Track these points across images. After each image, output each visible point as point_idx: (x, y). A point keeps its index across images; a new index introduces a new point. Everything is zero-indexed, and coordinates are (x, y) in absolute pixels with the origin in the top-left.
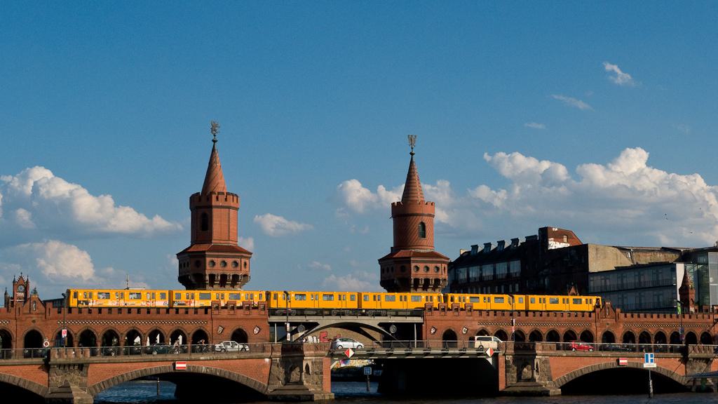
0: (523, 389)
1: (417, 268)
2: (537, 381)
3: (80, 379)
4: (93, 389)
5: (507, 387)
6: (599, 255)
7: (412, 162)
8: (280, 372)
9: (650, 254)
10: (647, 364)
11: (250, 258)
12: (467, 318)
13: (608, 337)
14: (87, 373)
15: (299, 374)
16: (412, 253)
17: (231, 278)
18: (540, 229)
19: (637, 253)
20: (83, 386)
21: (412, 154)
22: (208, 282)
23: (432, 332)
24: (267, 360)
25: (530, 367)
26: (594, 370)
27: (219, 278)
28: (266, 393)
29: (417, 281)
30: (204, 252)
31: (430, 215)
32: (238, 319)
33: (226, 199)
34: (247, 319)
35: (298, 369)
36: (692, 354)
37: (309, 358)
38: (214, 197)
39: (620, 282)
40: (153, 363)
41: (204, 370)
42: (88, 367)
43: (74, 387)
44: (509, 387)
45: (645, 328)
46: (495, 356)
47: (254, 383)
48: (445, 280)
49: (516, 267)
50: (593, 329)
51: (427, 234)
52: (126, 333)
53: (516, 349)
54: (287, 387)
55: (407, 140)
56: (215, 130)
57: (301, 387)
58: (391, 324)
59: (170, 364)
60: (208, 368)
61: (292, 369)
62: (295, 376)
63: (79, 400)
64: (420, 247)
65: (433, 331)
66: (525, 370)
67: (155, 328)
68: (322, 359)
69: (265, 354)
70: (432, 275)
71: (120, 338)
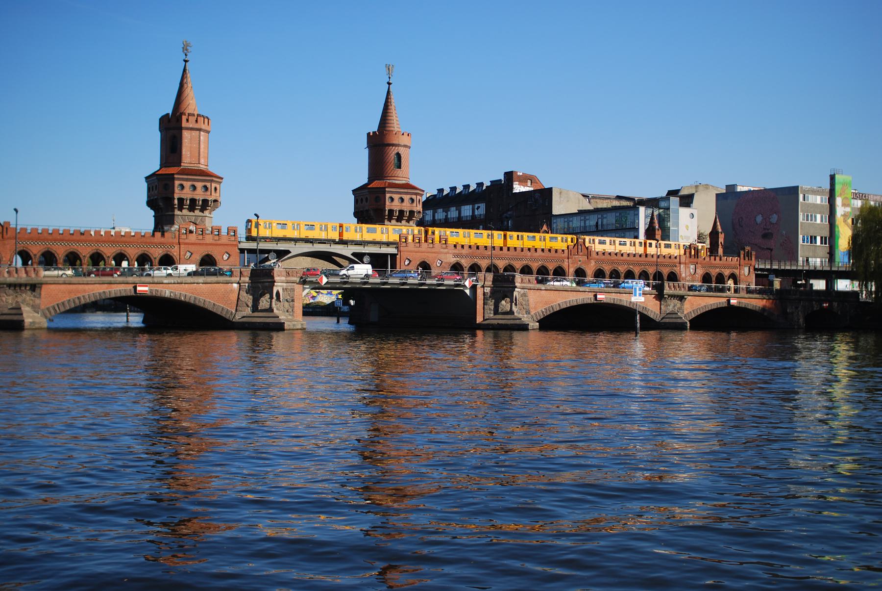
0: (501, 322)
1: (392, 199)
2: (515, 314)
3: (31, 300)
4: (47, 312)
5: (484, 320)
6: (562, 199)
7: (388, 92)
8: (248, 299)
9: (607, 201)
10: (635, 298)
11: (220, 183)
12: (442, 250)
13: (580, 273)
14: (40, 294)
15: (269, 300)
16: (387, 184)
17: (201, 202)
18: (506, 173)
19: (595, 200)
20: (35, 308)
21: (389, 84)
22: (176, 206)
23: (407, 263)
24: (236, 286)
25: (508, 299)
26: (572, 304)
27: (188, 202)
28: (234, 320)
29: (391, 211)
30: (173, 174)
31: (405, 146)
32: (206, 244)
33: (197, 121)
34: (217, 245)
35: (268, 296)
36: (667, 291)
37: (279, 284)
38: (184, 118)
39: (582, 224)
40: (113, 286)
41: (167, 295)
42: (41, 288)
43: (26, 309)
44: (487, 319)
45: (616, 266)
46: (474, 288)
47: (221, 309)
48: (419, 212)
49: (481, 210)
50: (565, 265)
51: (402, 166)
52: (88, 255)
53: (494, 281)
54: (256, 314)
55: (384, 71)
56: (187, 50)
57: (271, 314)
58: (364, 254)
59: (131, 287)
60: (171, 292)
61: (262, 295)
62: (264, 303)
63: (31, 323)
64: (395, 178)
65: (407, 262)
66: (503, 302)
67: (119, 251)
68: (294, 286)
69: (233, 279)
70: (406, 206)
71: (83, 261)
